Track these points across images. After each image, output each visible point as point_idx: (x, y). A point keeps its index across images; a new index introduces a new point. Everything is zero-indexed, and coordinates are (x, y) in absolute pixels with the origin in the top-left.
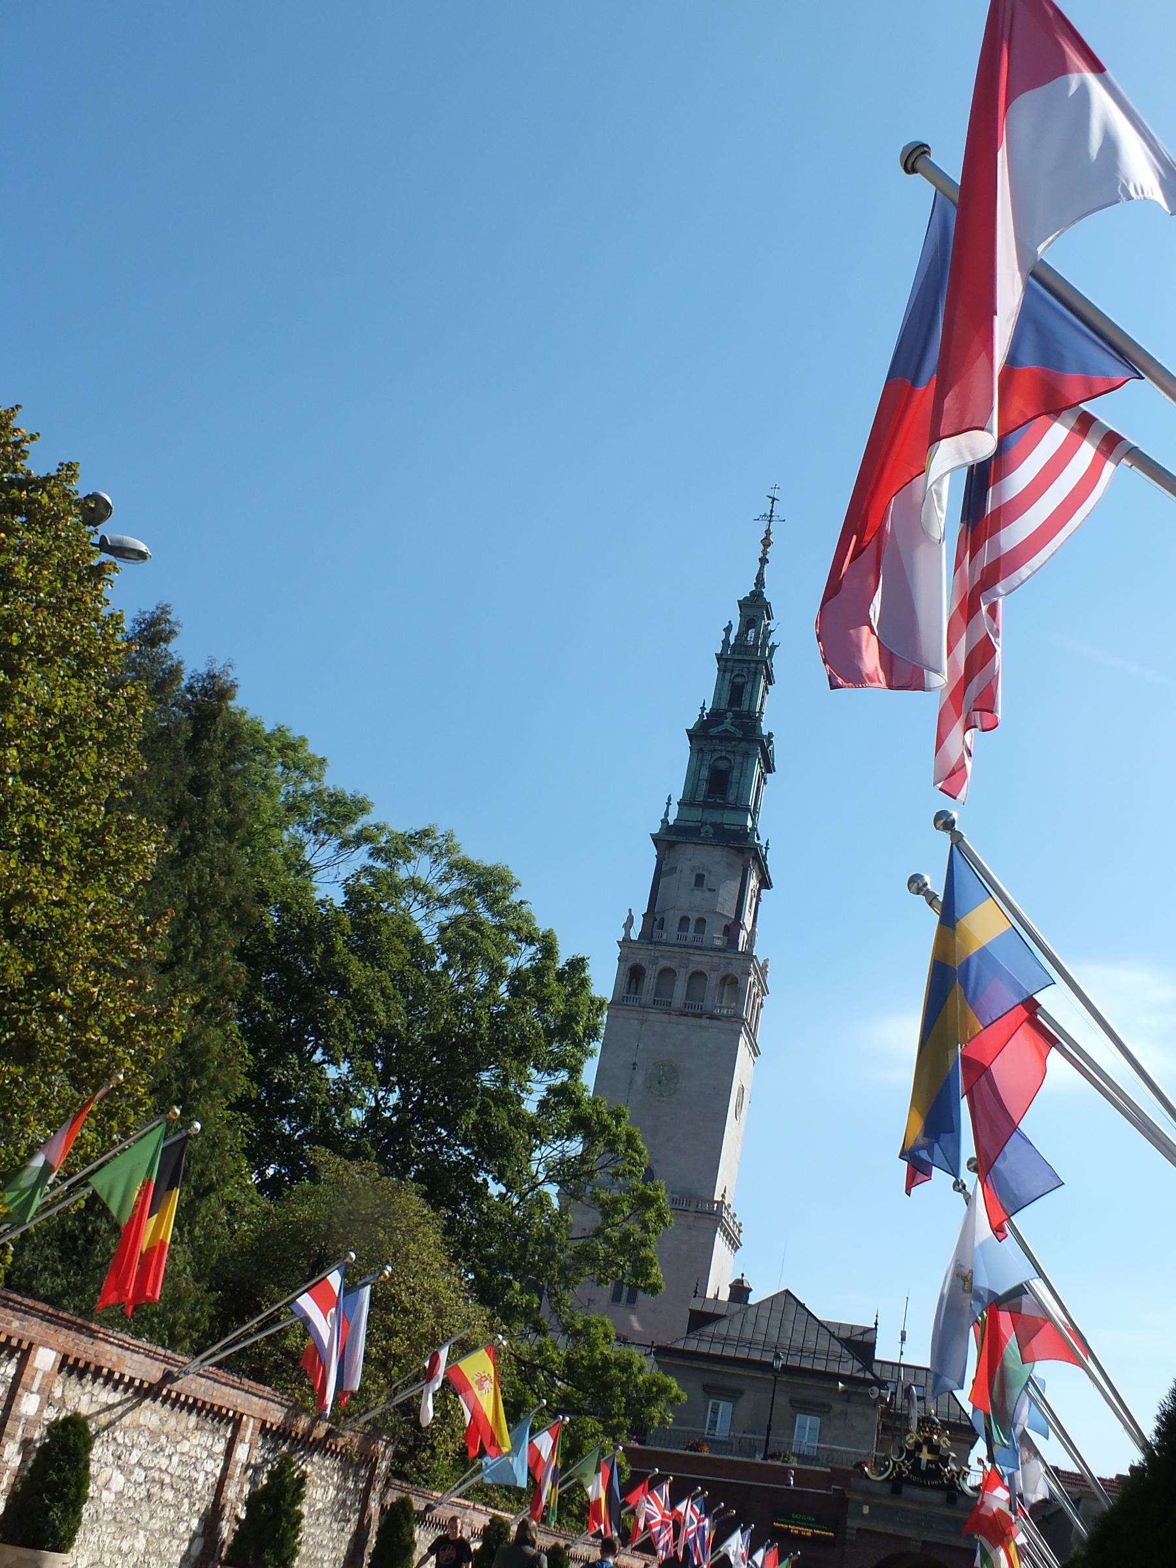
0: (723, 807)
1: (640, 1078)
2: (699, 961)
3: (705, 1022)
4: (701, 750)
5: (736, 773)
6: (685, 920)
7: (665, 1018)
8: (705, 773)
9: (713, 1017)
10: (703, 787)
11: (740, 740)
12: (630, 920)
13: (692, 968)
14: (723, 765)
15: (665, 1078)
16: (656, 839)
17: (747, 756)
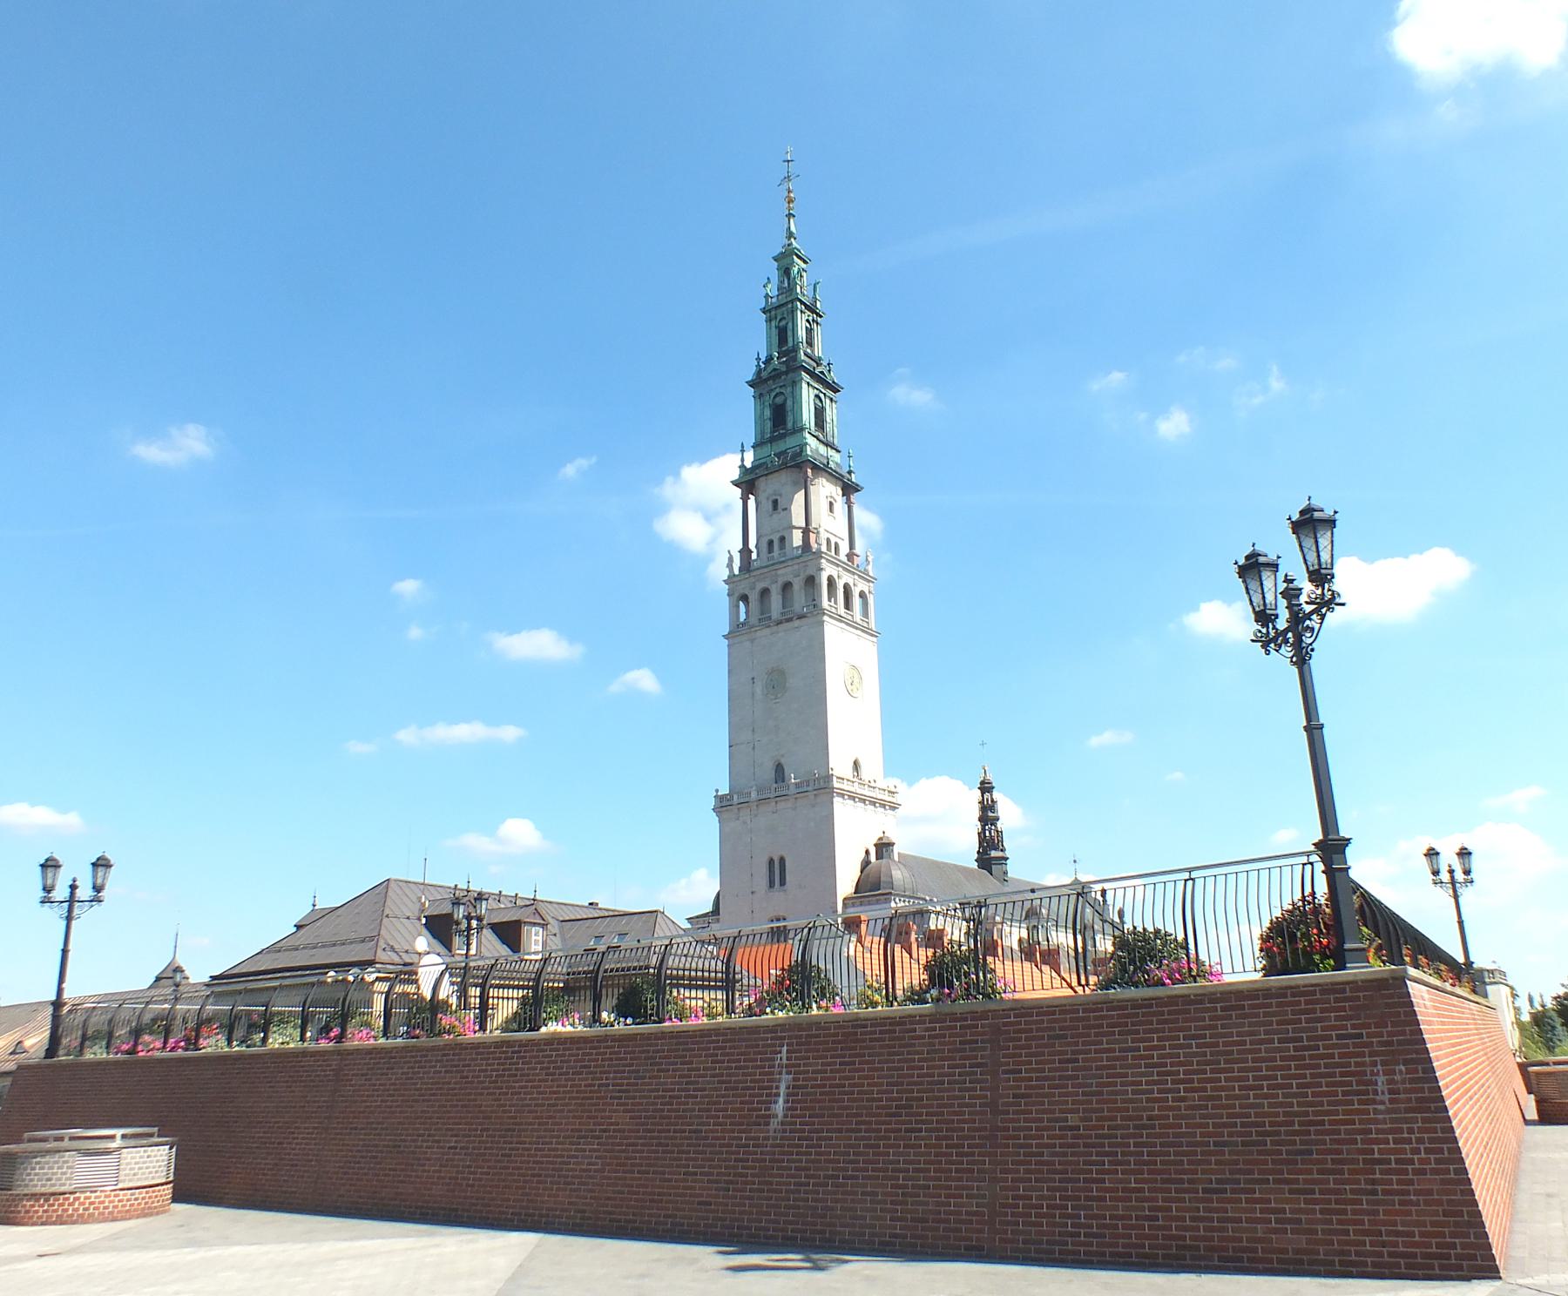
0: (783, 436)
1: (759, 690)
2: (785, 574)
3: (797, 623)
4: (761, 395)
5: (789, 403)
6: (771, 543)
7: (767, 631)
8: (768, 413)
9: (801, 617)
10: (769, 425)
11: (786, 373)
12: (731, 559)
13: (781, 581)
14: (779, 400)
15: (776, 682)
16: (736, 484)
17: (795, 384)
